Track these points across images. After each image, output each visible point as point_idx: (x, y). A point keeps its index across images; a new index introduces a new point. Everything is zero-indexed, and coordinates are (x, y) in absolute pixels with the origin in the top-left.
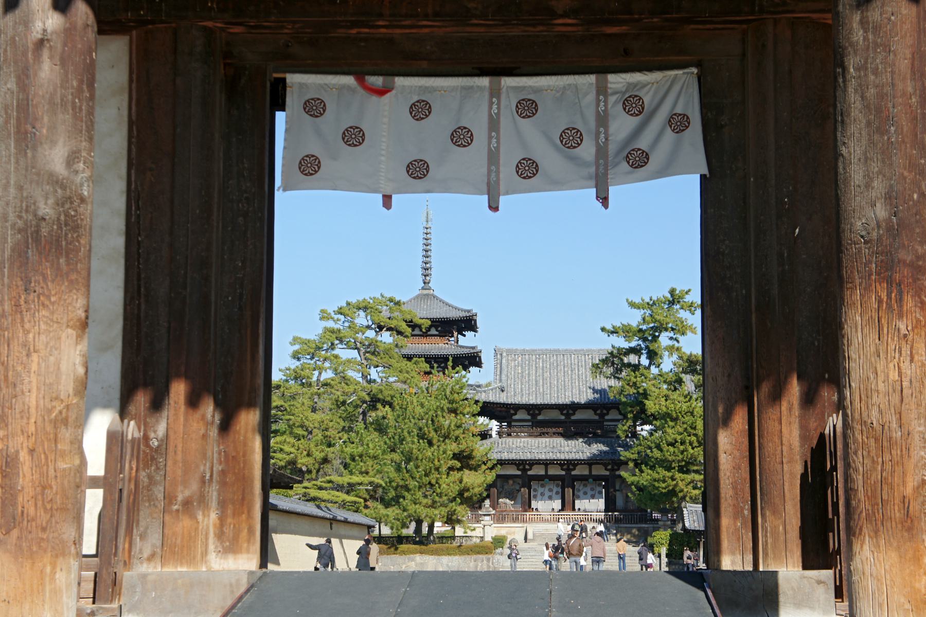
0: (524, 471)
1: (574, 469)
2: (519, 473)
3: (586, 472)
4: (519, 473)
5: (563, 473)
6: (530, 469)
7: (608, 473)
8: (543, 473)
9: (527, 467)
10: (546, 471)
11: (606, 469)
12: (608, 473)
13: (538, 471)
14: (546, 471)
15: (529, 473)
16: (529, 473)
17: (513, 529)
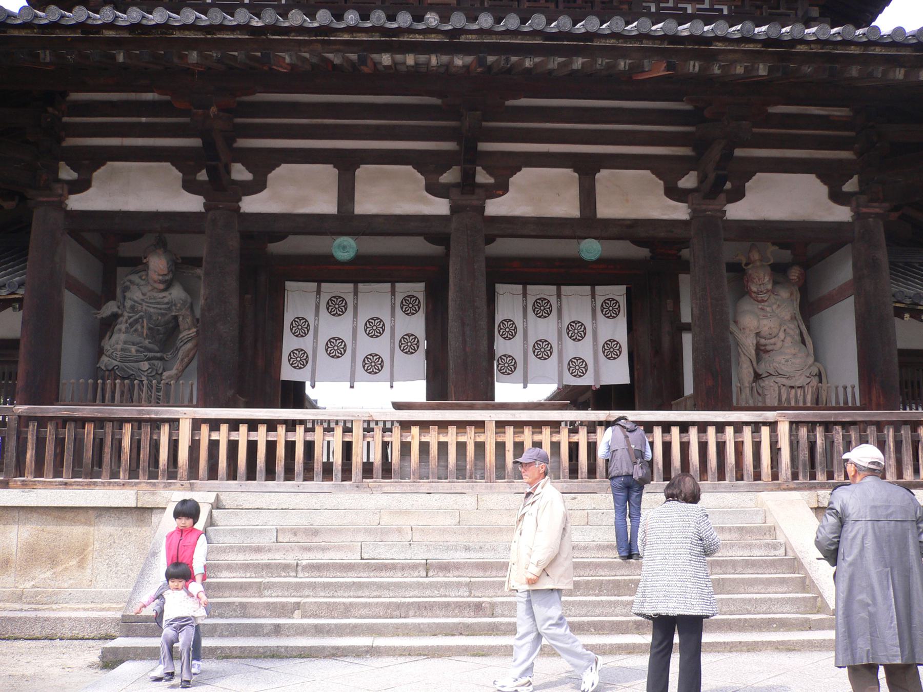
0: (221, 192)
1: (501, 188)
2: (193, 203)
3: (566, 206)
4: (193, 203)
5: (440, 207)
6: (258, 186)
7: (680, 212)
8: (327, 205)
9: (240, 173)
10: (346, 193)
11: (673, 192)
12: (680, 212)
13: (297, 191)
14: (346, 193)
15: (251, 204)
16: (251, 204)
17: (74, 532)
